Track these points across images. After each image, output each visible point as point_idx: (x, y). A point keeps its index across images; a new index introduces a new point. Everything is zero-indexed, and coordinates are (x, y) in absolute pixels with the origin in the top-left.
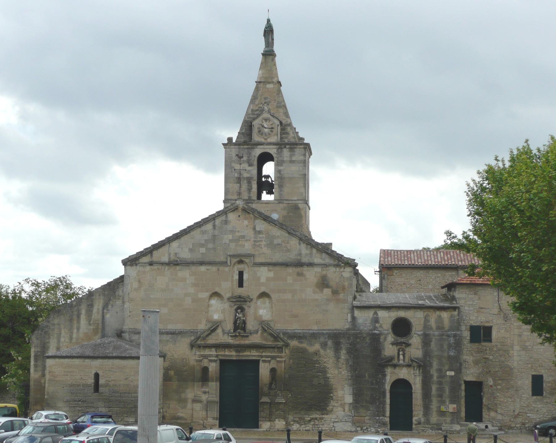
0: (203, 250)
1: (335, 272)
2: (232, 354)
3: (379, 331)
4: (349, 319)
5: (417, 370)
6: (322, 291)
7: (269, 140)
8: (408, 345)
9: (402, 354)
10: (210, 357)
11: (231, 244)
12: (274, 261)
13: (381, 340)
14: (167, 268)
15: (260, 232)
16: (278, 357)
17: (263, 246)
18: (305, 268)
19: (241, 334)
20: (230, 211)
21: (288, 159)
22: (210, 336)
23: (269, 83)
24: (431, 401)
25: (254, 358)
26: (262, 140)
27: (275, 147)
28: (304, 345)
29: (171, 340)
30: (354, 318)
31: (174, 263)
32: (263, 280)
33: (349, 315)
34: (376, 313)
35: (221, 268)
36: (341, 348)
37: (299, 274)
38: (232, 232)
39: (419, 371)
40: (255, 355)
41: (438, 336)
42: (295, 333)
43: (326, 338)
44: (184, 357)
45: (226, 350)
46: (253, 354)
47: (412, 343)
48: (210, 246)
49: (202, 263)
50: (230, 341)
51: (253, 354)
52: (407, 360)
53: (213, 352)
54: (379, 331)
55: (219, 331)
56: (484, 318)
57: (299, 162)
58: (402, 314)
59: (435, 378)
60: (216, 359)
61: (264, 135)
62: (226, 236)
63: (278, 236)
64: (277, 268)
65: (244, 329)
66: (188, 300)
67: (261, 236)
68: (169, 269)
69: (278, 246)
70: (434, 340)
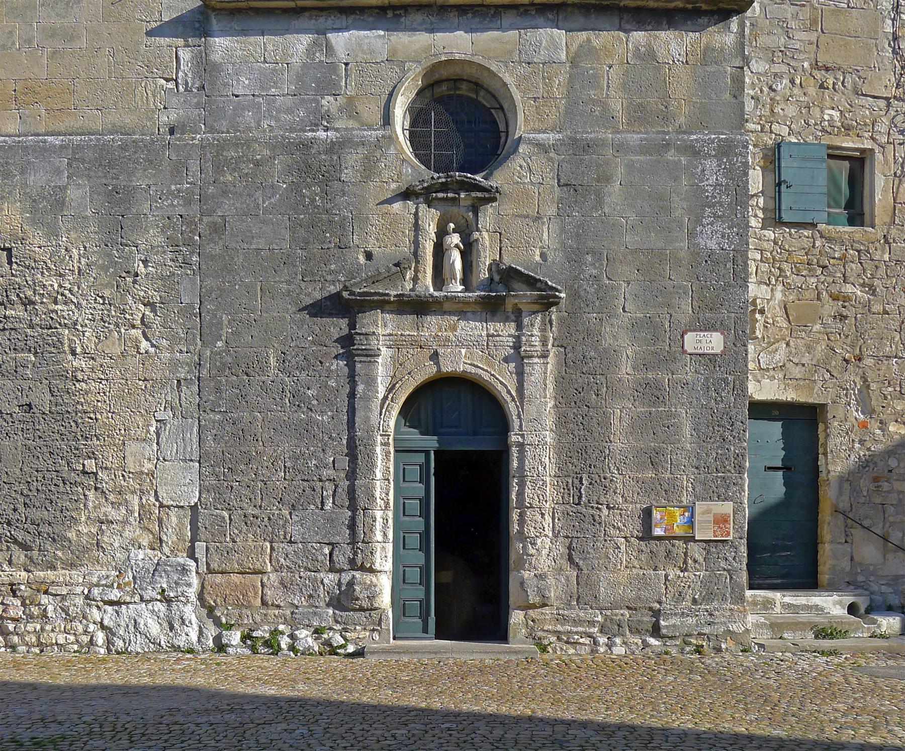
3: (337, 130)
8: (490, 196)
13: (347, 175)
24: (603, 484)
41: (643, 150)
43: (58, 172)
47: (506, 188)
54: (337, 130)
59: (625, 370)
70: (620, 172)
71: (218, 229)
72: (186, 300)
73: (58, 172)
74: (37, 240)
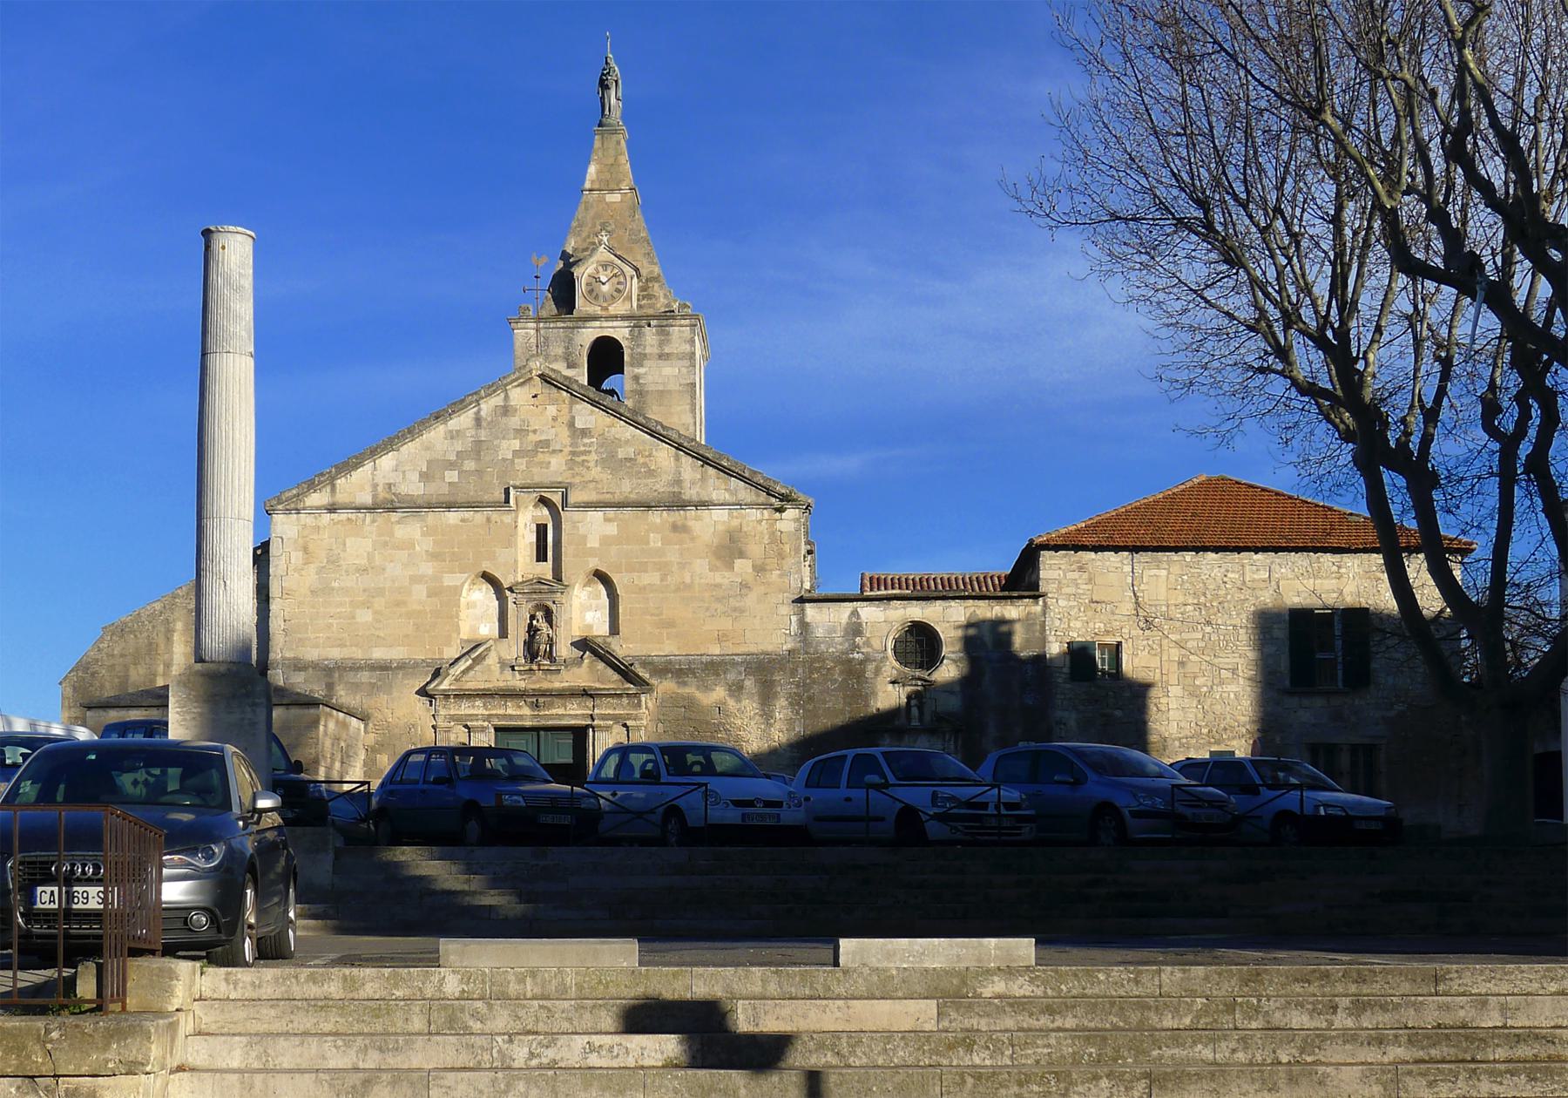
0: (452, 476)
1: (760, 522)
2: (521, 713)
4: (794, 627)
5: (950, 740)
6: (730, 567)
7: (612, 310)
9: (916, 705)
10: (472, 721)
11: (516, 461)
12: (617, 498)
13: (869, 674)
14: (369, 517)
15: (585, 433)
16: (629, 717)
17: (592, 464)
18: (691, 512)
19: (542, 668)
20: (515, 384)
21: (656, 351)
22: (472, 673)
23: (612, 191)
25: (573, 722)
26: (596, 310)
27: (626, 324)
28: (691, 690)
29: (379, 683)
30: (804, 626)
31: (387, 505)
32: (593, 543)
33: (794, 618)
34: (855, 613)
35: (495, 516)
36: (776, 695)
37: (675, 528)
38: (521, 432)
39: (956, 742)
40: (576, 715)
42: (670, 662)
43: (740, 673)
44: (412, 721)
45: (508, 704)
46: (572, 712)
48: (470, 465)
49: (450, 506)
50: (517, 682)
51: (572, 713)
52: (927, 717)
53: (478, 708)
54: (863, 653)
55: (492, 660)
56: (1102, 625)
57: (681, 357)
58: (917, 612)
60: (486, 724)
61: (601, 299)
62: (505, 443)
63: (627, 442)
64: (627, 513)
65: (550, 656)
66: (420, 592)
67: (586, 441)
68: (373, 521)
69: (628, 464)
71: (810, 699)
72: (797, 729)
73: (740, 673)
74: (731, 703)
